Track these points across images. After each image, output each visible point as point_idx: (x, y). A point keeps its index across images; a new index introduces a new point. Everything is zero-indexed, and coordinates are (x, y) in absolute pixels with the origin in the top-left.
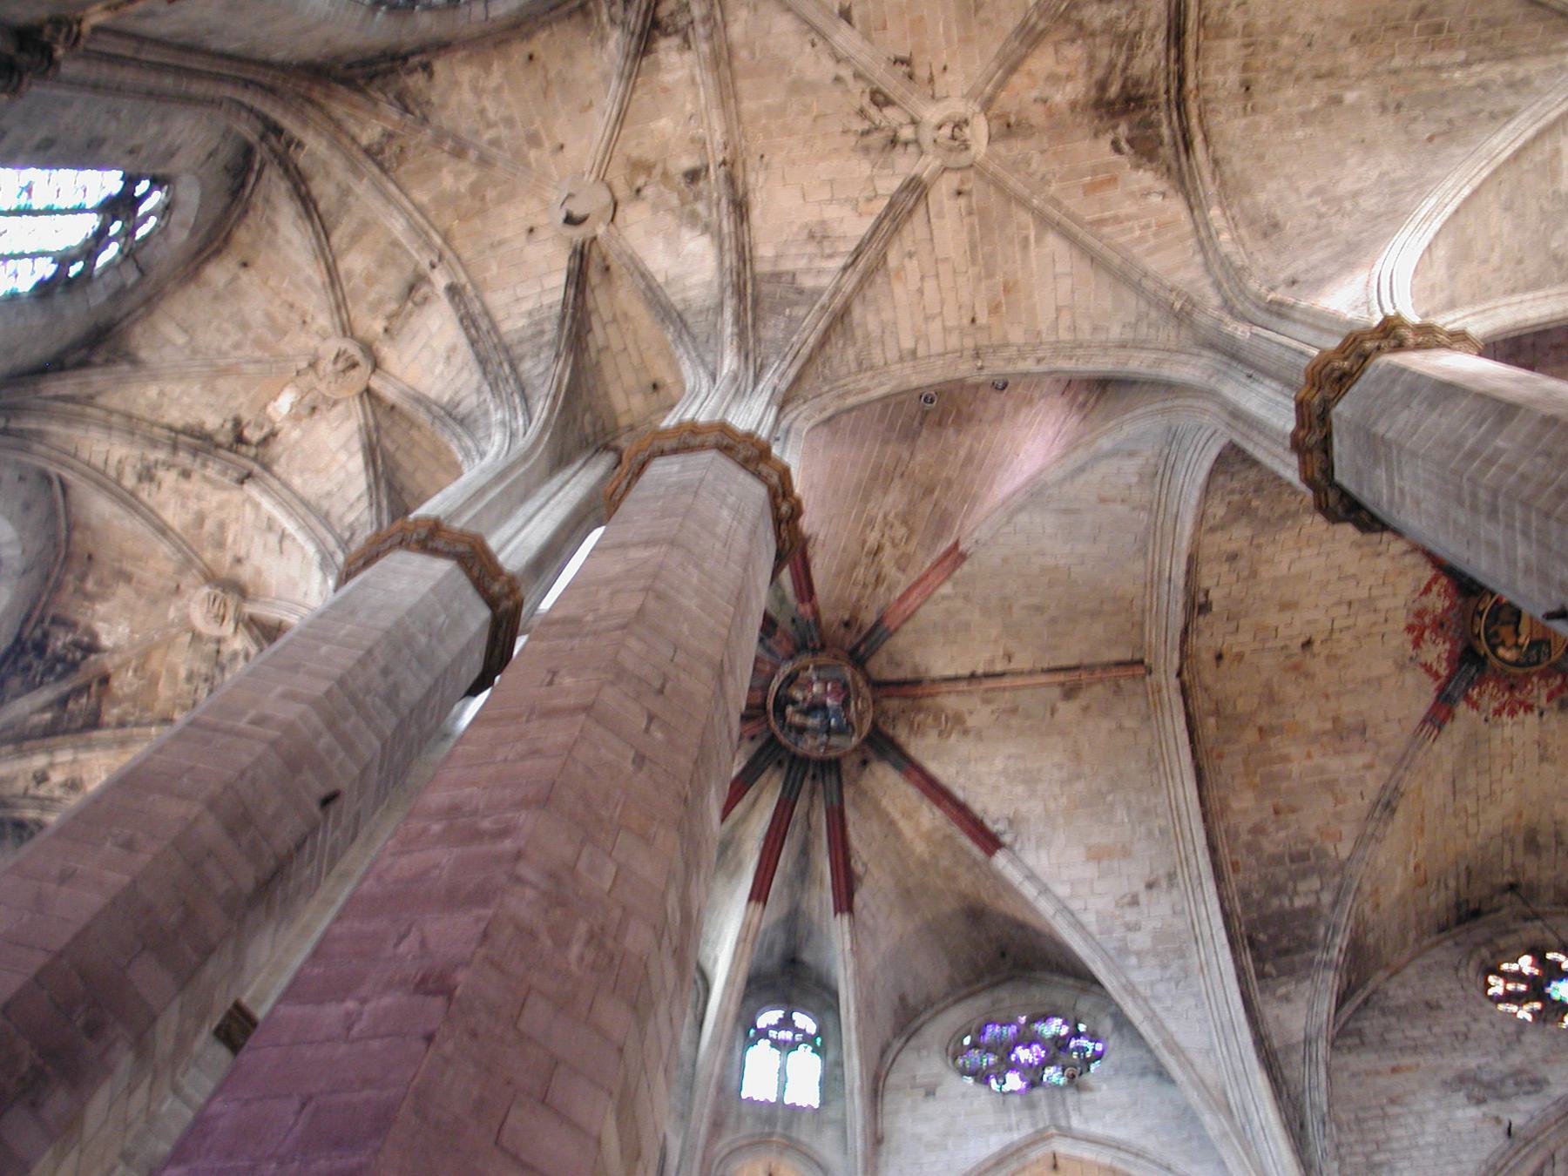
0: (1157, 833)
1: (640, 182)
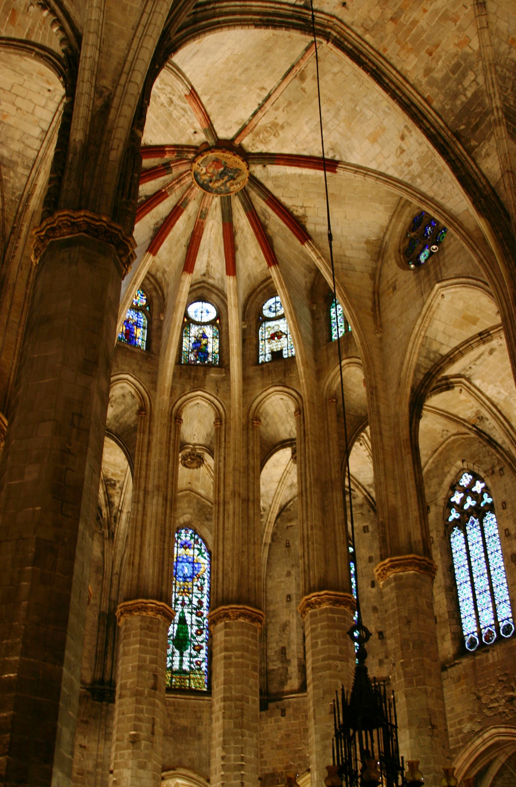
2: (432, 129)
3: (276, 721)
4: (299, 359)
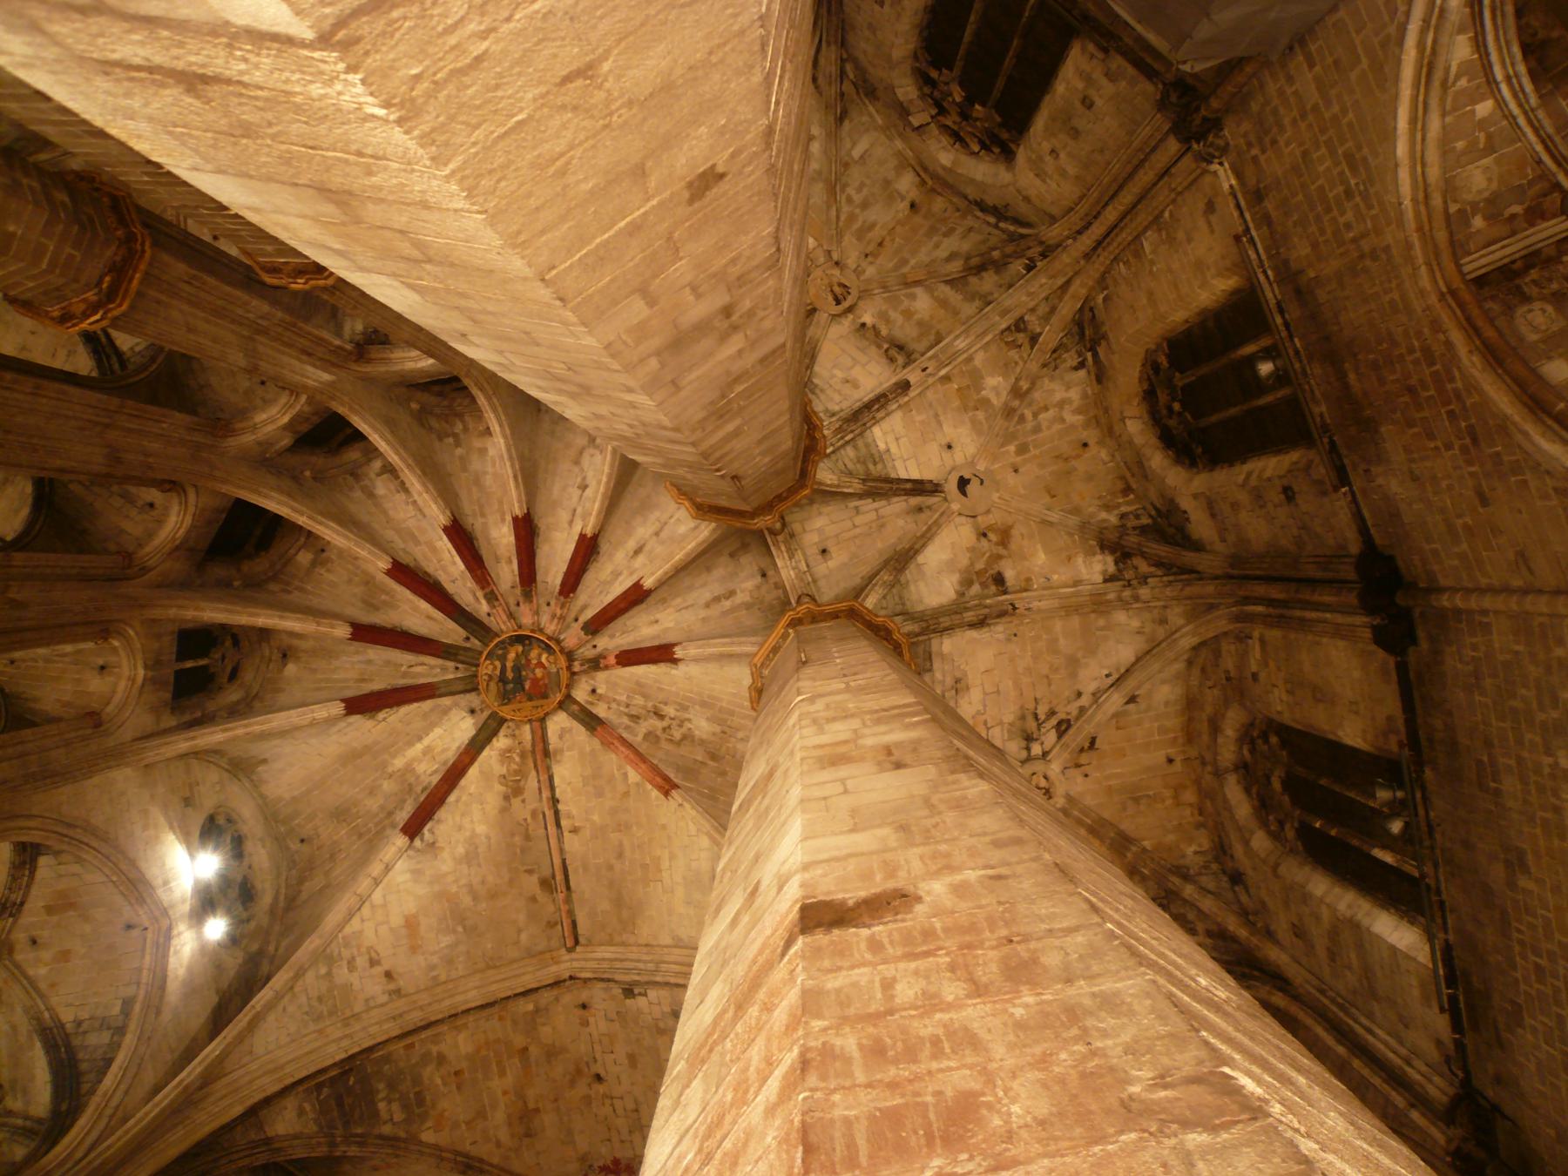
0: (434, 973)
1: (992, 536)
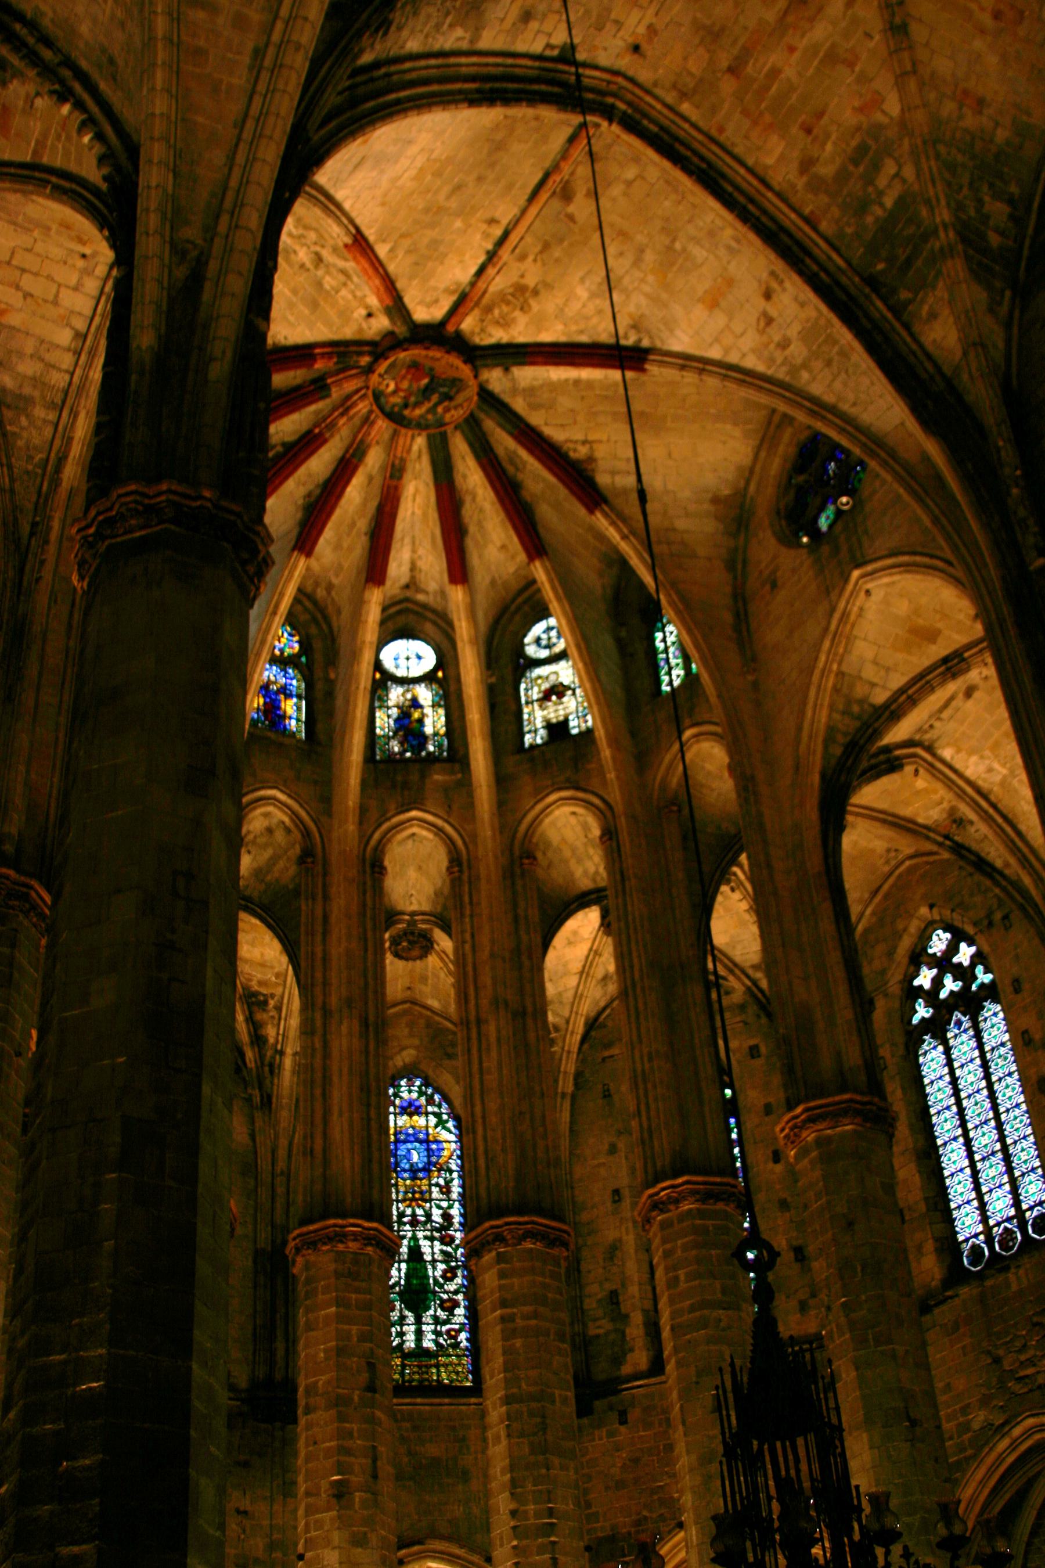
0: (733, 244)
2: (823, 275)
3: (611, 1434)
4: (600, 734)
